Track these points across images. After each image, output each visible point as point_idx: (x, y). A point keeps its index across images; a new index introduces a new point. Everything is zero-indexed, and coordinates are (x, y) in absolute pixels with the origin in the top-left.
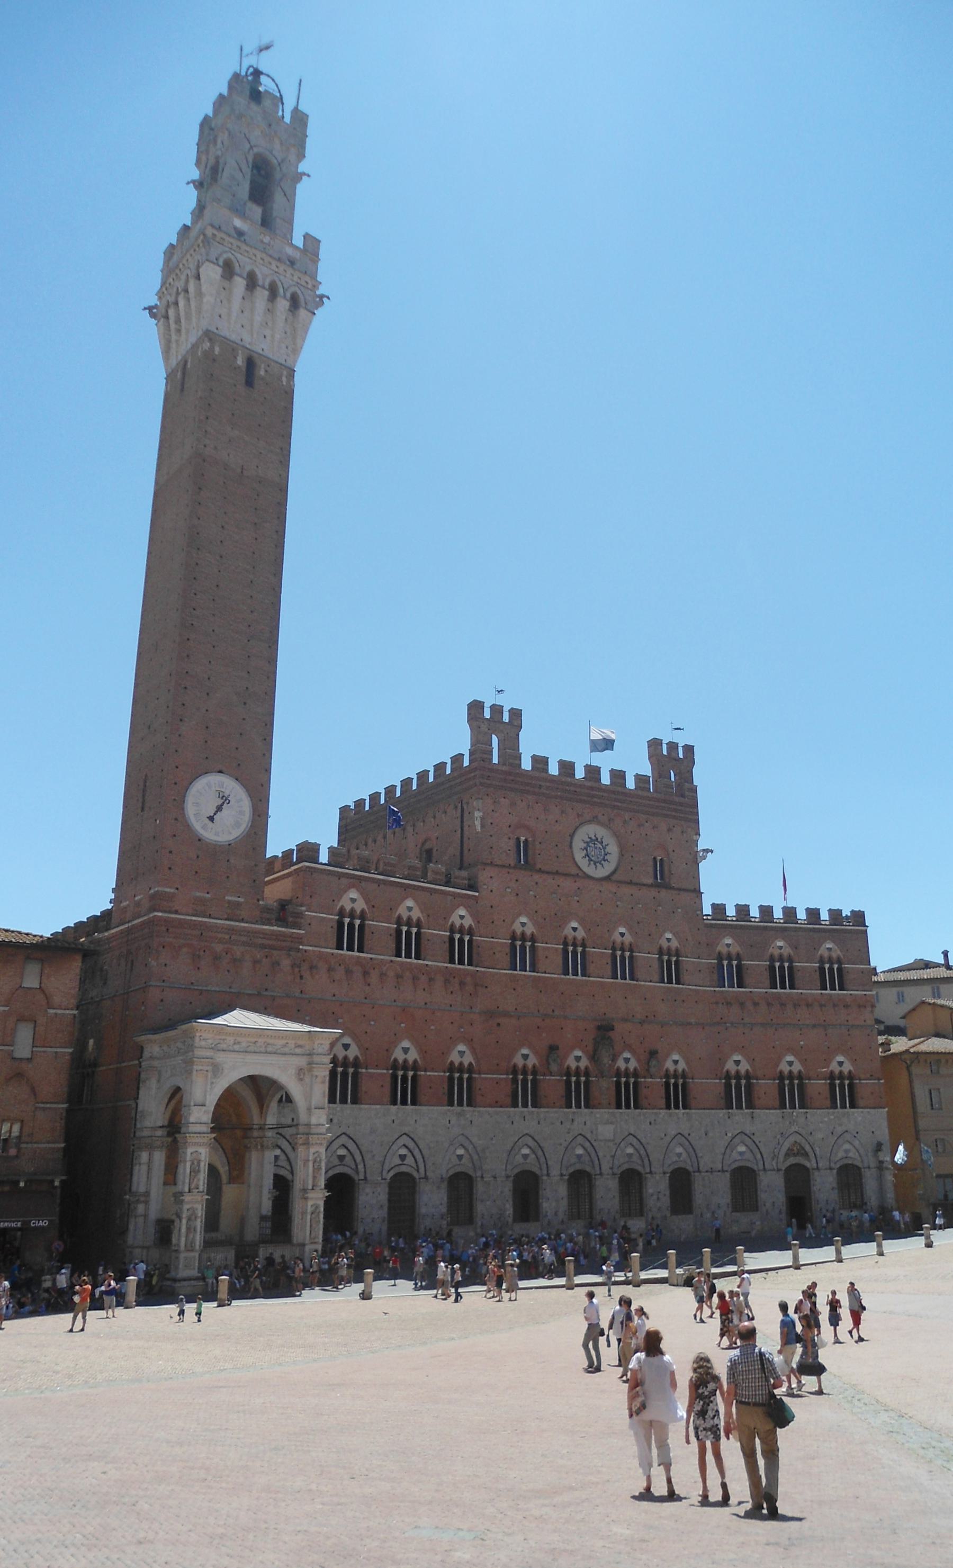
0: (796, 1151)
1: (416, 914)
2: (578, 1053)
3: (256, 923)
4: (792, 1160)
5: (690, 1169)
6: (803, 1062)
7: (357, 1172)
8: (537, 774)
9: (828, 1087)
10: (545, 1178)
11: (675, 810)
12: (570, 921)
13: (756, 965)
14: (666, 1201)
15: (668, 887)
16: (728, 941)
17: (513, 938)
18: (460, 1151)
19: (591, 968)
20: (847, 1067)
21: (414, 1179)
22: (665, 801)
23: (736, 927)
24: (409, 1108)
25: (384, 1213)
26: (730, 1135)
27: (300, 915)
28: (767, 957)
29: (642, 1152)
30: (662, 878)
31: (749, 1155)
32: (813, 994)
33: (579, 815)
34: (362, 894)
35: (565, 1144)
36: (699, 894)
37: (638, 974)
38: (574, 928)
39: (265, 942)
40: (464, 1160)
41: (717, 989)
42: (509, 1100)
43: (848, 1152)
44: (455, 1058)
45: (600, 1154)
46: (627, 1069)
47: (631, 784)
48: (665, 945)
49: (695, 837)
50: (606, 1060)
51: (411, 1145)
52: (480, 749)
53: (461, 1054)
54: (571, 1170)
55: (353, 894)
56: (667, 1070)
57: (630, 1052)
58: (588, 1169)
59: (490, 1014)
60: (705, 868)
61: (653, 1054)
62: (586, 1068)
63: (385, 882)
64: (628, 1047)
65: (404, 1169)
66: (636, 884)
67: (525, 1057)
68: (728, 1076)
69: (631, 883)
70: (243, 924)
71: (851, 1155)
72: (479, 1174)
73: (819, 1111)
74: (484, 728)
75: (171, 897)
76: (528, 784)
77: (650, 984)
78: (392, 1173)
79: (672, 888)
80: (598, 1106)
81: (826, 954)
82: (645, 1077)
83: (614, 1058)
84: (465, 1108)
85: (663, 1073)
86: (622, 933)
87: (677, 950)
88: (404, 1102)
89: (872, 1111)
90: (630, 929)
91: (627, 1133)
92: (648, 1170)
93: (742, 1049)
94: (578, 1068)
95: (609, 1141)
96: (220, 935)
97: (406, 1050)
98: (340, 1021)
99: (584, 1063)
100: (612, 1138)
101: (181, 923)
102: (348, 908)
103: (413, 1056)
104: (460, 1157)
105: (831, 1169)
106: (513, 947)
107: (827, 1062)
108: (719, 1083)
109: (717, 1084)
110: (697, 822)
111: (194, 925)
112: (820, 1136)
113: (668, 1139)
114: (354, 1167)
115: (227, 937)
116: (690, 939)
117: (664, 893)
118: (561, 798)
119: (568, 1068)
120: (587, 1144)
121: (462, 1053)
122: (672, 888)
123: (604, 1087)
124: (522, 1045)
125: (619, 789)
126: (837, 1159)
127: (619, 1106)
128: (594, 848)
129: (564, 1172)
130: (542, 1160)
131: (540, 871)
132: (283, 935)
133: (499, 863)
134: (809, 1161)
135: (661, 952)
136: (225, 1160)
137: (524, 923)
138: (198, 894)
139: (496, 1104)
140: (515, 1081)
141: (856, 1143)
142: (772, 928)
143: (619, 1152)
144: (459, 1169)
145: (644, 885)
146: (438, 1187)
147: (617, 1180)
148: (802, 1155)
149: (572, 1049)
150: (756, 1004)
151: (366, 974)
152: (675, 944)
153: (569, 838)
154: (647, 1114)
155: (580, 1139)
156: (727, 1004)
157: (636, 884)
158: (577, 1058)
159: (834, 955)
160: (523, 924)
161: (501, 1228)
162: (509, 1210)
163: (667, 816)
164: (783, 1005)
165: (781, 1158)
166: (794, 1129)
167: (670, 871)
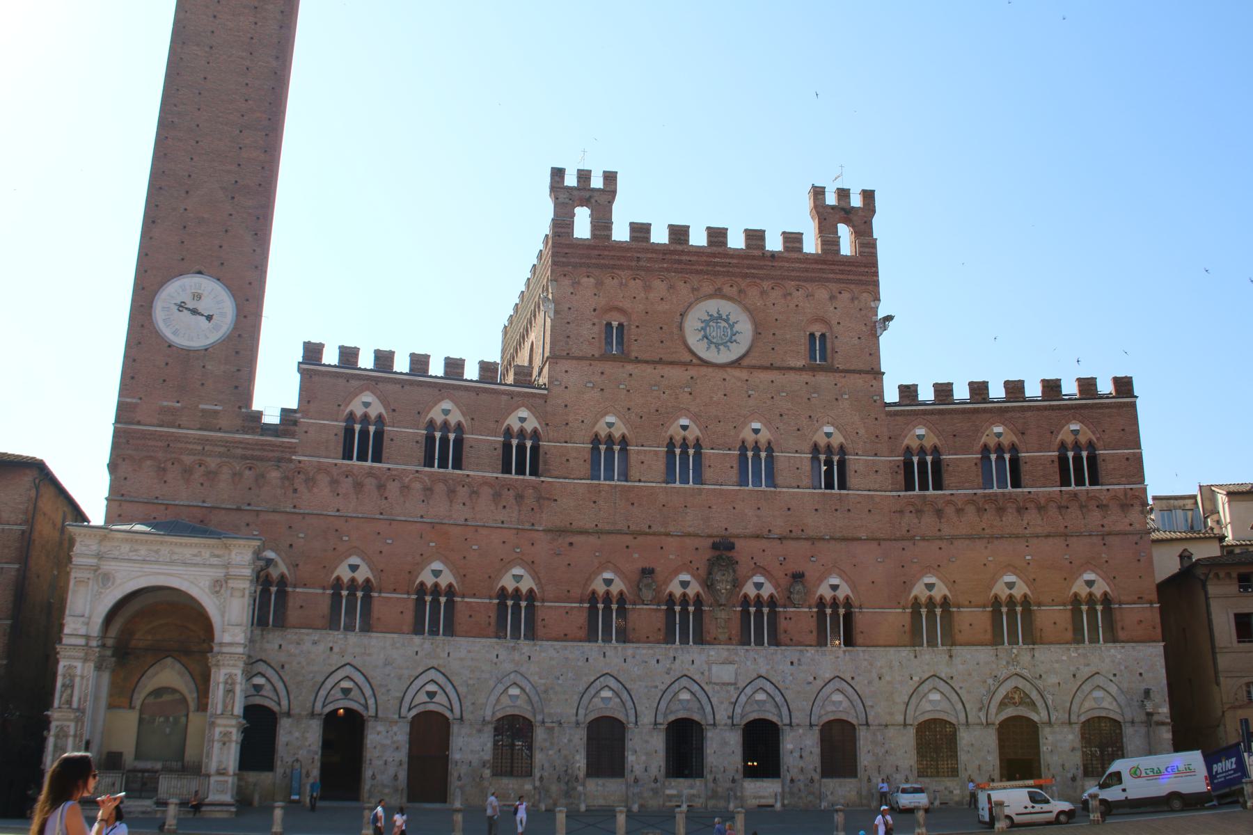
0: (1017, 700)
1: (455, 417)
2: (685, 577)
3: (237, 431)
4: (1010, 712)
5: (854, 721)
6: (1031, 582)
7: (366, 707)
8: (634, 245)
9: (1069, 614)
10: (631, 725)
11: (842, 272)
12: (678, 418)
13: (959, 459)
14: (813, 759)
15: (831, 369)
16: (921, 431)
17: (596, 440)
18: (514, 691)
19: (708, 474)
20: (1100, 588)
21: (447, 719)
22: (824, 262)
23: (932, 412)
24: (441, 637)
25: (403, 755)
26: (916, 678)
27: (295, 423)
28: (978, 447)
29: (779, 698)
30: (823, 358)
31: (945, 705)
32: (1049, 493)
33: (694, 290)
34: (378, 398)
35: (664, 687)
36: (878, 374)
37: (779, 480)
38: (684, 425)
39: (250, 452)
40: (519, 702)
41: (902, 494)
42: (582, 633)
43: (1103, 702)
44: (508, 583)
45: (714, 700)
46: (758, 596)
47: (774, 244)
48: (822, 442)
49: (873, 304)
50: (723, 587)
51: (441, 680)
52: (562, 224)
53: (516, 578)
54: (672, 718)
55: (368, 397)
56: (821, 598)
57: (763, 575)
58: (696, 717)
60: (886, 341)
61: (798, 577)
62: (698, 595)
63: (411, 383)
64: (759, 569)
65: (431, 707)
66: (779, 369)
67: (608, 582)
68: (916, 604)
69: (771, 367)
70: (220, 434)
71: (1105, 704)
72: (539, 718)
73: (1053, 648)
74: (563, 197)
75: (133, 407)
76: (619, 258)
77: (798, 489)
78: (414, 712)
79: (837, 370)
80: (715, 641)
81: (1070, 439)
82: (785, 606)
83: (737, 584)
84: (522, 641)
86: (756, 429)
87: (841, 447)
88: (434, 632)
89: (1140, 647)
90: (768, 423)
91: (755, 676)
92: (787, 721)
93: (937, 568)
94: (684, 595)
95: (728, 684)
96: (191, 447)
97: (437, 573)
98: (346, 538)
99: (694, 589)
100: (733, 681)
101: (144, 435)
102: (359, 412)
103: (446, 579)
105: (1070, 723)
106: (595, 450)
107: (1070, 578)
108: (904, 617)
109: (898, 617)
110: (876, 284)
111: (161, 436)
112: (1053, 680)
113: (820, 683)
114: (363, 701)
115: (200, 448)
116: (862, 431)
117: (822, 379)
118: (667, 270)
119: (671, 595)
120: (696, 688)
121: (518, 578)
122: (837, 370)
123: (723, 619)
124: (602, 567)
125: (757, 253)
126: (1083, 710)
127: (745, 642)
128: (717, 327)
129: (660, 720)
130: (629, 704)
131: (637, 361)
132: (271, 445)
133: (581, 354)
134: (1038, 713)
135: (816, 449)
136: (192, 685)
137: (612, 423)
138: (165, 404)
139: (565, 638)
140: (593, 610)
141: (1113, 689)
142: (985, 410)
143: (743, 698)
144: (510, 712)
145: (791, 369)
146: (480, 731)
147: (740, 732)
148: (1027, 705)
149: (677, 572)
150: (959, 511)
151: (381, 487)
152: (837, 440)
153: (678, 318)
154: (791, 653)
155: (684, 682)
156: (918, 511)
157: (779, 369)
159: (1083, 439)
160: (610, 425)
161: (567, 783)
162: (580, 762)
163: (828, 280)
164: (1001, 511)
165: (993, 710)
166: (1012, 670)
167: (833, 349)
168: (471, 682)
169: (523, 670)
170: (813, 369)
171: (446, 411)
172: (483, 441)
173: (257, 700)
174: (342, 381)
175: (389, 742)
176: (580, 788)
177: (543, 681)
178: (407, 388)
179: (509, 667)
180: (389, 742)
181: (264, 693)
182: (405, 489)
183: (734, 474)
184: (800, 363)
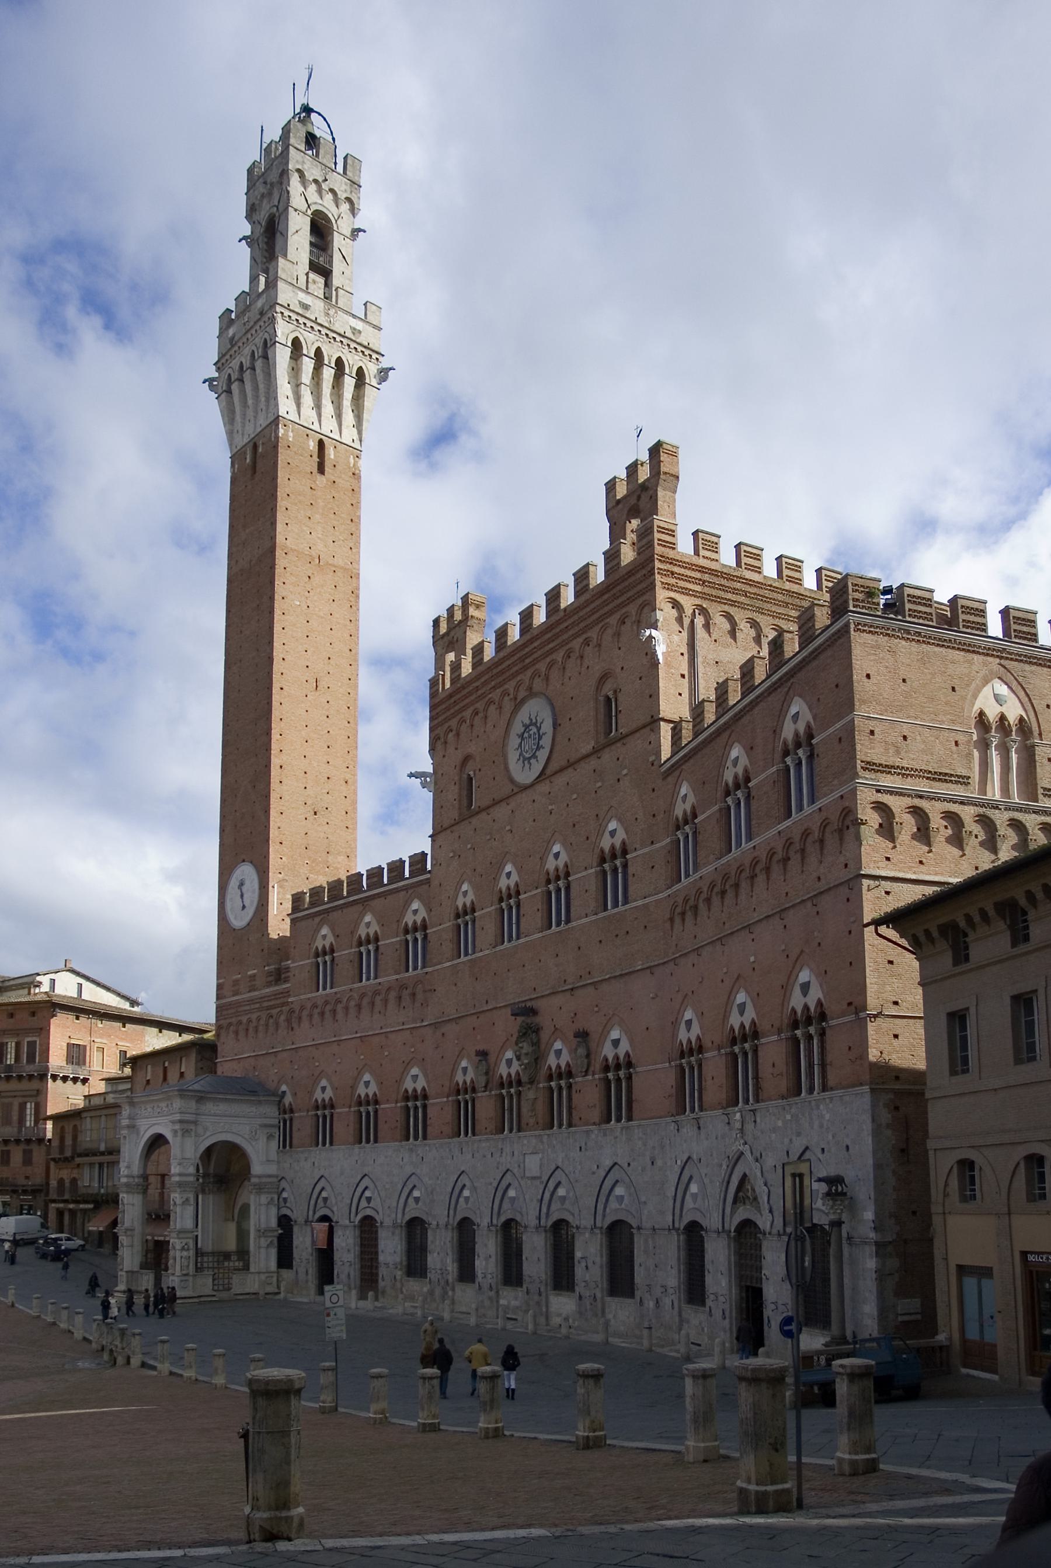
18: (416, 1193)
26: (679, 1162)
35: (495, 1185)
41: (669, 892)
44: (409, 1085)
53: (415, 1080)
59: (435, 1025)
61: (583, 1035)
65: (369, 1212)
83: (538, 1058)
85: (597, 1065)
88: (368, 1141)
100: (538, 1175)
101: (230, 1004)
103: (373, 1089)
104: (417, 1200)
139: (441, 1135)
143: (547, 1195)
146: (393, 1233)
149: (503, 1049)
158: (508, 1064)
168: (387, 1186)
169: (418, 1172)
170: (596, 751)
171: (369, 923)
172: (390, 941)
173: (285, 1211)
174: (310, 920)
175: (344, 1244)
176: (450, 1293)
177: (430, 1182)
178: (345, 911)
179: (409, 1170)
180: (344, 1244)
181: (288, 1205)
182: (347, 1008)
183: (538, 919)
184: (587, 748)
